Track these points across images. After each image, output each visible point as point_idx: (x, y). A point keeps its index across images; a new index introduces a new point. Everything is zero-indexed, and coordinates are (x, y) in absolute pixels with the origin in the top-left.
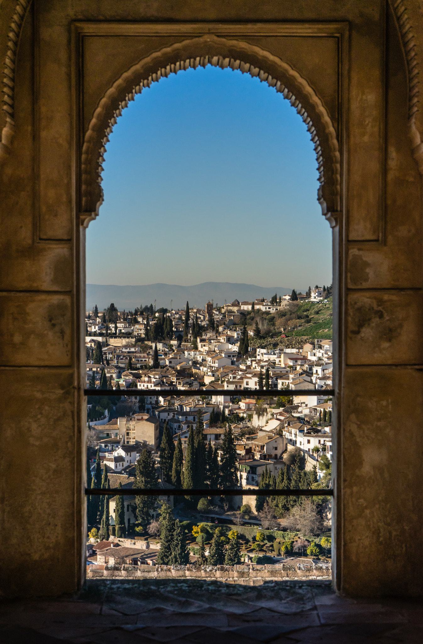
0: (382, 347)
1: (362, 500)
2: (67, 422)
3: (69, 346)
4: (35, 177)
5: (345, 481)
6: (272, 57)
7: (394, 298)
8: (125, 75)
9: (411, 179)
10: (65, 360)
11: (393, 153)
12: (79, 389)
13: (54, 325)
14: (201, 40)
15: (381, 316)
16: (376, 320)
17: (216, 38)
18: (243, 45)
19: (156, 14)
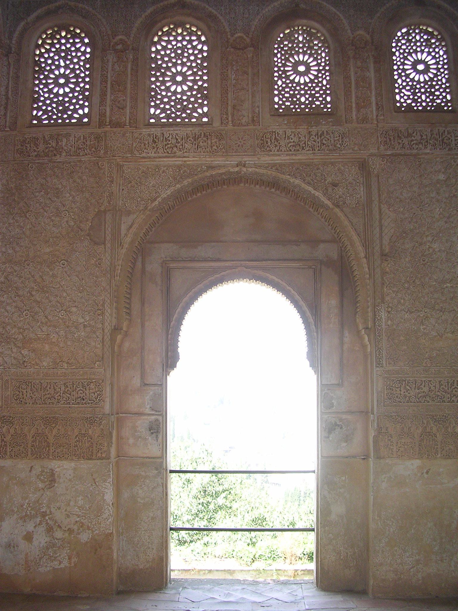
0: (342, 446)
1: (331, 535)
2: (160, 489)
3: (161, 445)
4: (143, 348)
5: (321, 523)
6: (276, 279)
7: (349, 417)
8: (193, 290)
9: (357, 349)
10: (159, 454)
11: (346, 333)
12: (167, 470)
13: (152, 433)
14: (237, 270)
15: (341, 428)
16: (338, 430)
17: (245, 269)
18: (260, 273)
19: (211, 257)
